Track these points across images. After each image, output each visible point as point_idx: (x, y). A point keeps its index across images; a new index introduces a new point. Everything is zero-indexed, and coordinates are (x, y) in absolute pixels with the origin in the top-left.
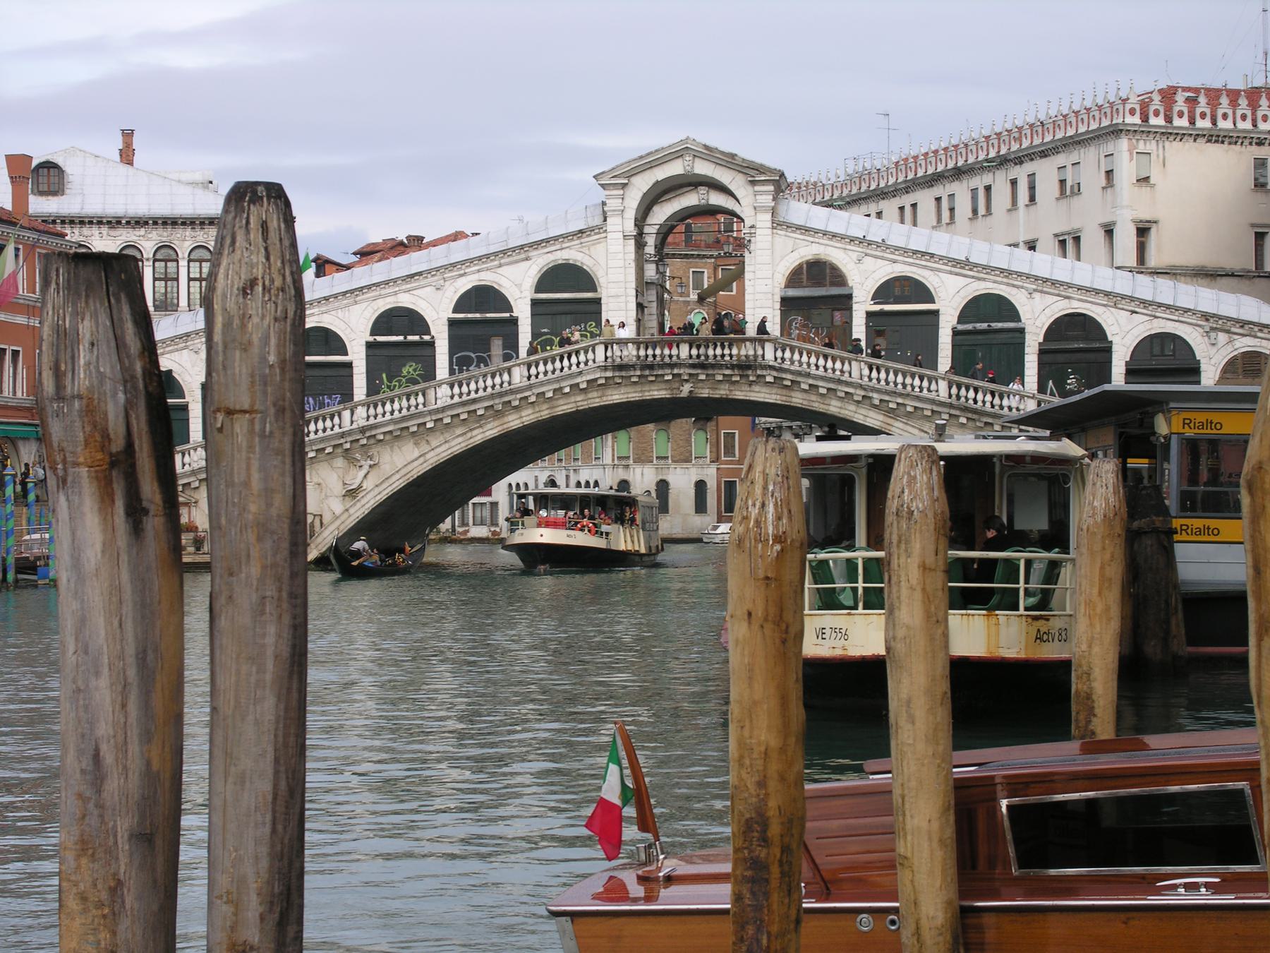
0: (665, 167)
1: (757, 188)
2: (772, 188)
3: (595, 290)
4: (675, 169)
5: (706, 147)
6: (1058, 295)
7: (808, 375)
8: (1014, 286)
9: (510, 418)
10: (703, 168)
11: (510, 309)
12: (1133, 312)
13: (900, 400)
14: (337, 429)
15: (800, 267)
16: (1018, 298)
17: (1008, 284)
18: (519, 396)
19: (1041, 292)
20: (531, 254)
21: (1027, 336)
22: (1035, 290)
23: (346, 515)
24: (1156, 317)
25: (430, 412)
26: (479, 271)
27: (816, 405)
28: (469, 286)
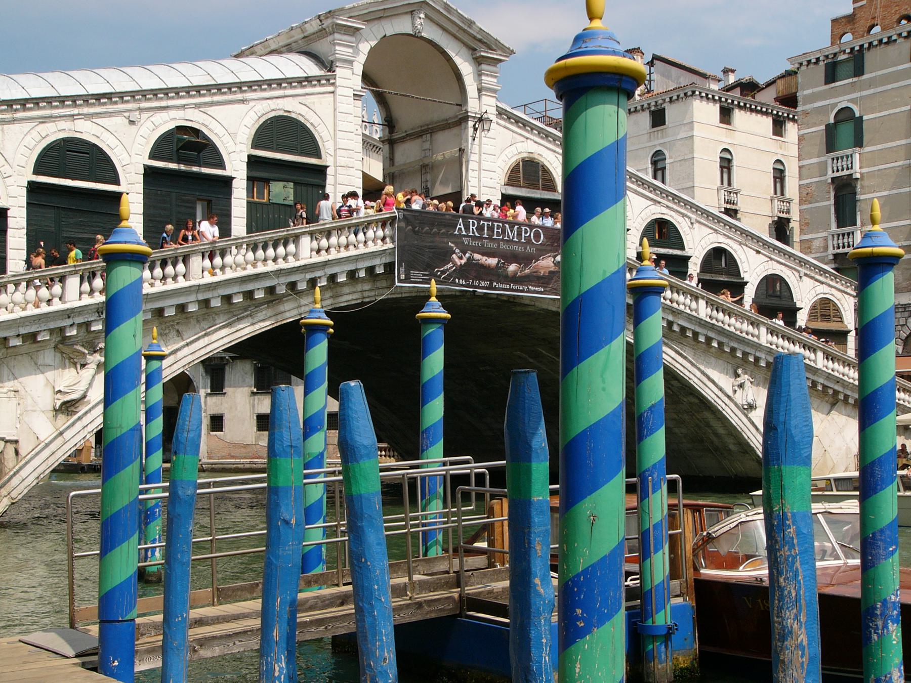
1: (484, 66)
3: (318, 155)
4: (402, 26)
5: (447, 7)
9: (287, 306)
10: (430, 32)
11: (222, 165)
12: (758, 252)
14: (57, 306)
15: (518, 164)
16: (682, 225)
18: (309, 276)
23: (59, 441)
24: (771, 259)
25: (199, 288)
26: (183, 107)
28: (172, 126)
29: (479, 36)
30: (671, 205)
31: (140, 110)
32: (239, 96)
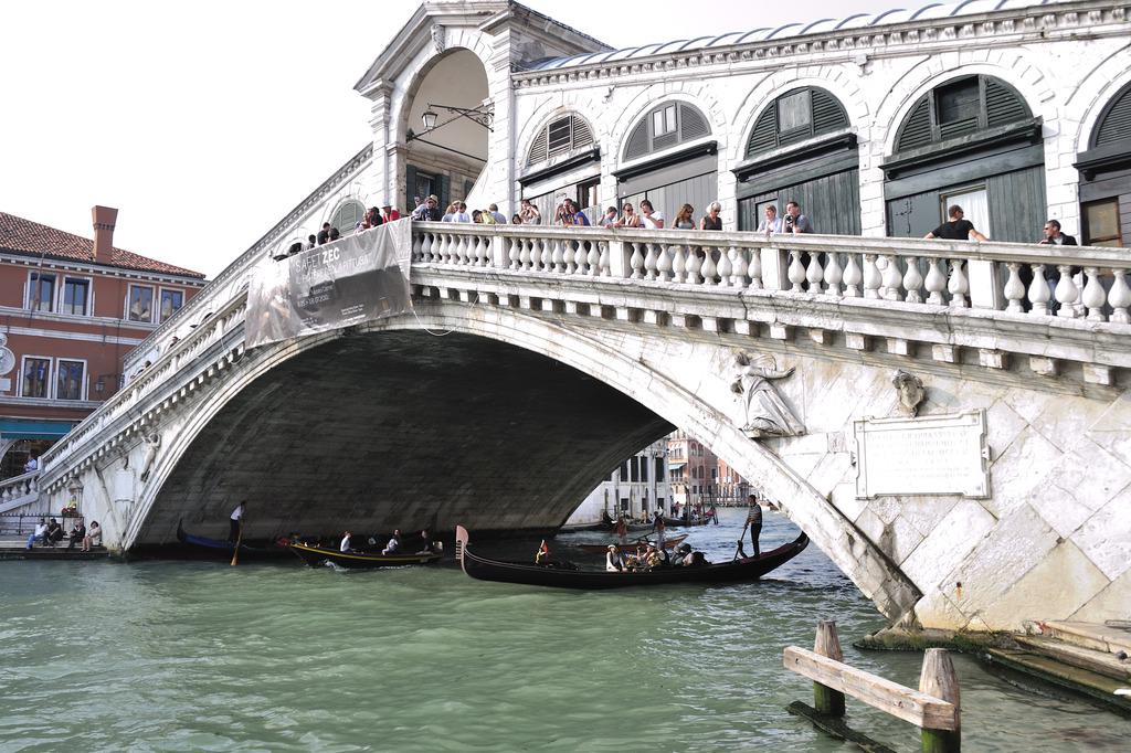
0: (422, 52)
2: (507, 32)
4: (431, 51)
5: (440, 6)
6: (918, 53)
7: (438, 273)
8: (833, 62)
10: (454, 39)
12: (1093, 37)
13: (554, 294)
17: (822, 64)
19: (885, 56)
20: (324, 199)
21: (865, 155)
22: (869, 58)
26: (293, 229)
27: (470, 324)
29: (476, 12)
30: (806, 58)
31: (274, 245)
32: (319, 203)
